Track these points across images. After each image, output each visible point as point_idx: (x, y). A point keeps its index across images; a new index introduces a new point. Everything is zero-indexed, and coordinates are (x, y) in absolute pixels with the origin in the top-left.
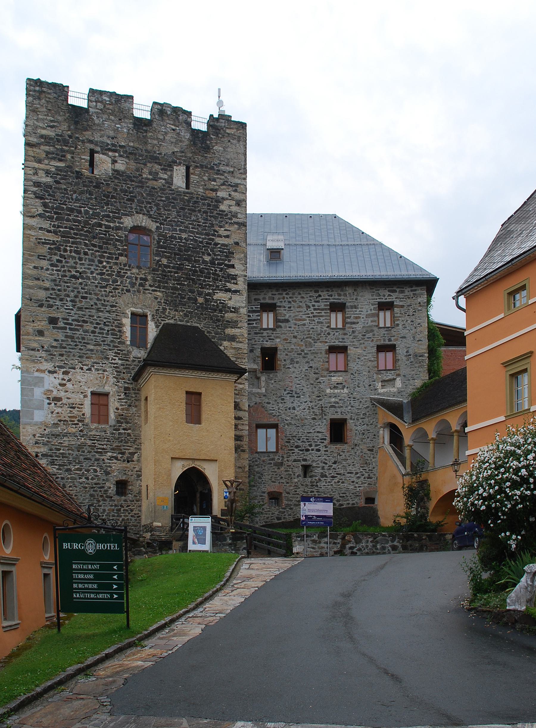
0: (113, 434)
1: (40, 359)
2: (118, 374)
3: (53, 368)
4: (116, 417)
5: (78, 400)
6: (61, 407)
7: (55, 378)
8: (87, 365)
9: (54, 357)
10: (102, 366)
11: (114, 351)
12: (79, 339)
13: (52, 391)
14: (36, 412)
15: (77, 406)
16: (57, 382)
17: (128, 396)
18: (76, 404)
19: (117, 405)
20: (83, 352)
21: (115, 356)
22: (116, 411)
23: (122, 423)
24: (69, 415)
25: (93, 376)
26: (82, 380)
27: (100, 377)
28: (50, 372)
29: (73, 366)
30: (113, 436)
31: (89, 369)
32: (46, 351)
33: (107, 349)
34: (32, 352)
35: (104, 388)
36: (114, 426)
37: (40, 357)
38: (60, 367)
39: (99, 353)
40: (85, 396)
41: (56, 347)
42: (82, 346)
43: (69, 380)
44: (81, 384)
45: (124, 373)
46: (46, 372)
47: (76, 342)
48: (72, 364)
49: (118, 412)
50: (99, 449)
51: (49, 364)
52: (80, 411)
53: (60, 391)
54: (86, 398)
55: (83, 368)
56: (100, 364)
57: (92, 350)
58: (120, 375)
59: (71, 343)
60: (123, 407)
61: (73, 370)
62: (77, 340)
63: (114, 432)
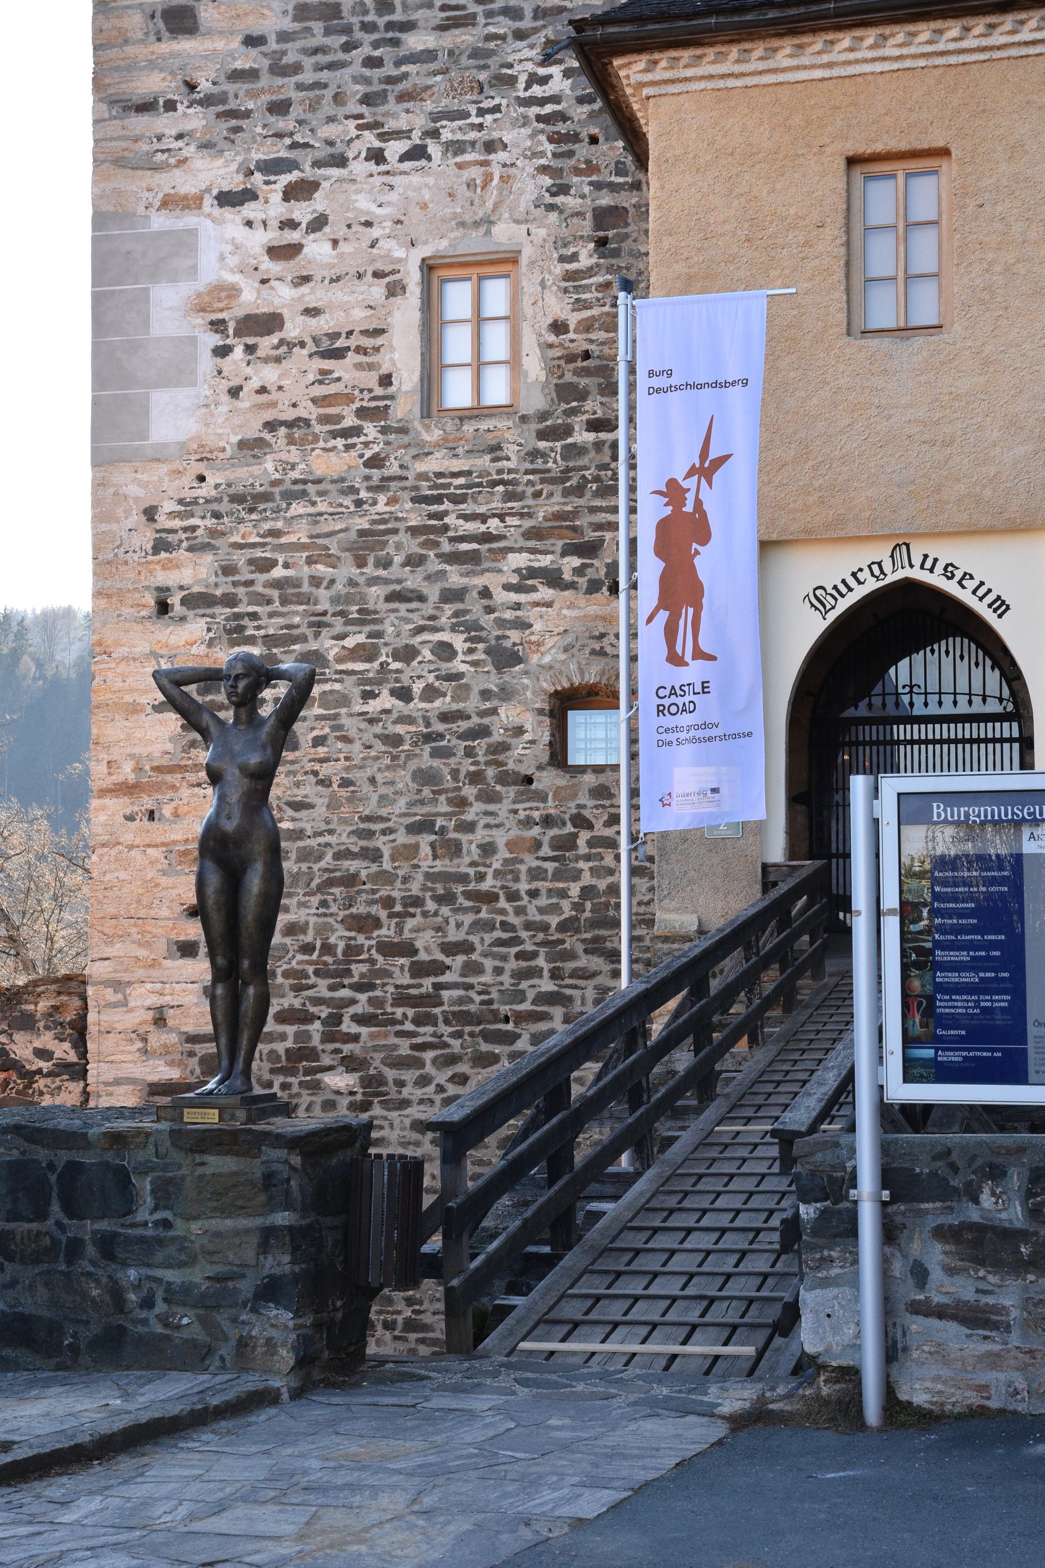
0: (535, 454)
1: (180, 144)
2: (564, 148)
3: (241, 177)
4: (550, 371)
5: (359, 313)
6: (278, 360)
7: (249, 224)
8: (406, 134)
9: (244, 123)
10: (480, 127)
11: (540, 38)
12: (366, 12)
13: (234, 291)
14: (161, 400)
15: (352, 342)
16: (259, 239)
17: (616, 253)
18: (350, 333)
19: (558, 307)
20: (377, 73)
21: (543, 64)
22: (552, 338)
23: (582, 395)
24: (319, 391)
25: (431, 181)
26: (379, 211)
27: (471, 185)
28: (228, 199)
29: (339, 148)
30: (539, 464)
31: (417, 153)
32: (207, 101)
33: (503, 38)
34: (140, 123)
35: (488, 232)
36: (543, 416)
37: (180, 137)
38: (272, 167)
39: (465, 61)
40: (395, 290)
41: (252, 74)
42: (376, 45)
43: (319, 223)
44: (375, 232)
45: (594, 140)
46: (208, 201)
47: (347, 30)
48: (331, 143)
49: (561, 345)
50: (462, 539)
51: (220, 162)
52: (371, 367)
53: (273, 283)
54: (398, 300)
55: (381, 150)
56: (466, 115)
57: (428, 56)
58: (570, 154)
59: (328, 41)
60: (587, 314)
61: (335, 172)
62: (355, 20)
63: (542, 445)
